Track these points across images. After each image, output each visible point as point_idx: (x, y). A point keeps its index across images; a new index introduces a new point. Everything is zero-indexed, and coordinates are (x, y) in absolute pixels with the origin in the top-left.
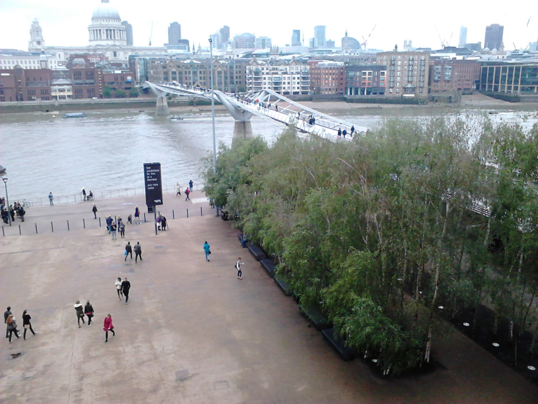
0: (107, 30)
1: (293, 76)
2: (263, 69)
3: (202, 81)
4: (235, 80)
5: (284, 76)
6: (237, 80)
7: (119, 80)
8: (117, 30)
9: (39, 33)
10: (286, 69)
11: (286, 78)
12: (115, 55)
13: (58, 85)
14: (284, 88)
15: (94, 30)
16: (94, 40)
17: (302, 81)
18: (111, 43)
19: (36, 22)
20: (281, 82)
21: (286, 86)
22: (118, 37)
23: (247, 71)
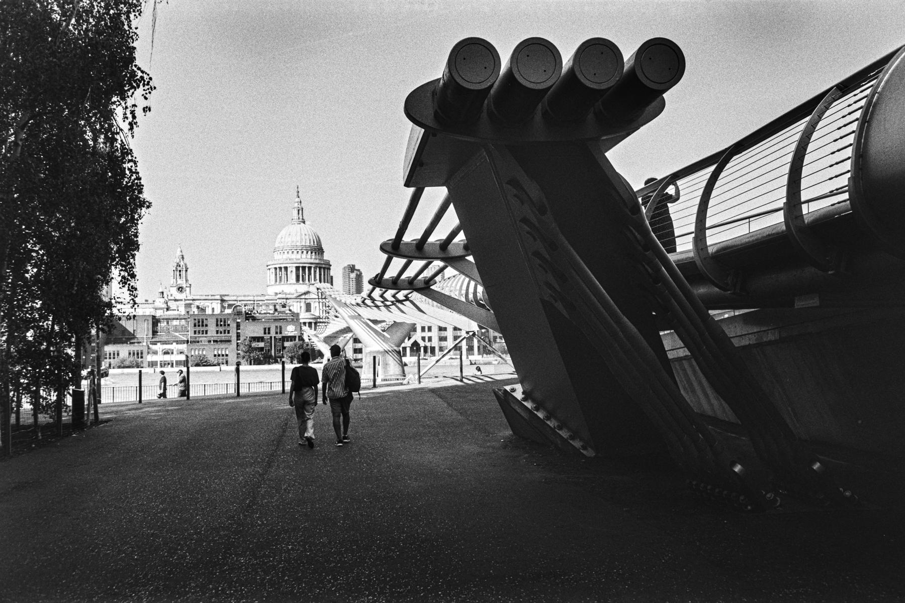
3: (427, 334)
7: (273, 334)
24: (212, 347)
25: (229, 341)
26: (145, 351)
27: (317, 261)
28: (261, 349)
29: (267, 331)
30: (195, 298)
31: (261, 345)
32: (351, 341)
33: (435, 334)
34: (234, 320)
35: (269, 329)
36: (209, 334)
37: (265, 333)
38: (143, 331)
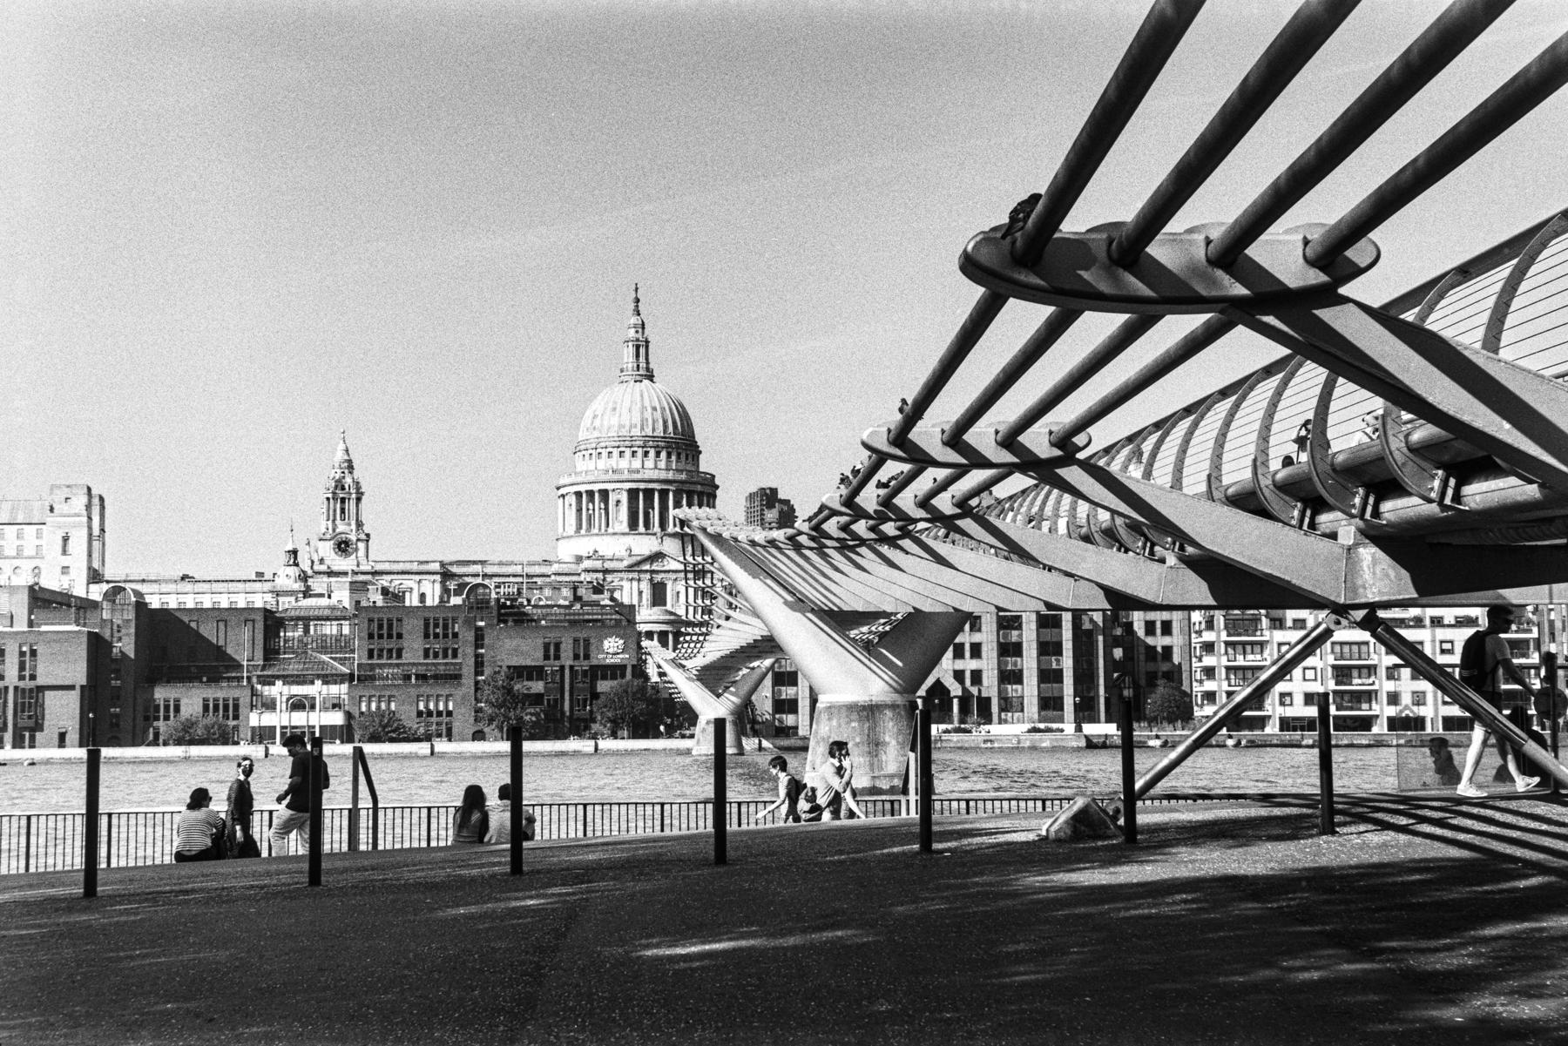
0: (633, 494)
1: (1442, 634)
3: (969, 664)
7: (567, 660)
12: (658, 596)
13: (289, 680)
14: (1394, 699)
15: (579, 494)
18: (644, 545)
24: (413, 692)
25: (457, 677)
26: (245, 700)
27: (683, 477)
28: (537, 699)
29: (552, 650)
30: (379, 567)
31: (538, 687)
32: (768, 681)
33: (988, 663)
34: (469, 622)
35: (557, 646)
36: (407, 657)
37: (547, 657)
38: (243, 647)
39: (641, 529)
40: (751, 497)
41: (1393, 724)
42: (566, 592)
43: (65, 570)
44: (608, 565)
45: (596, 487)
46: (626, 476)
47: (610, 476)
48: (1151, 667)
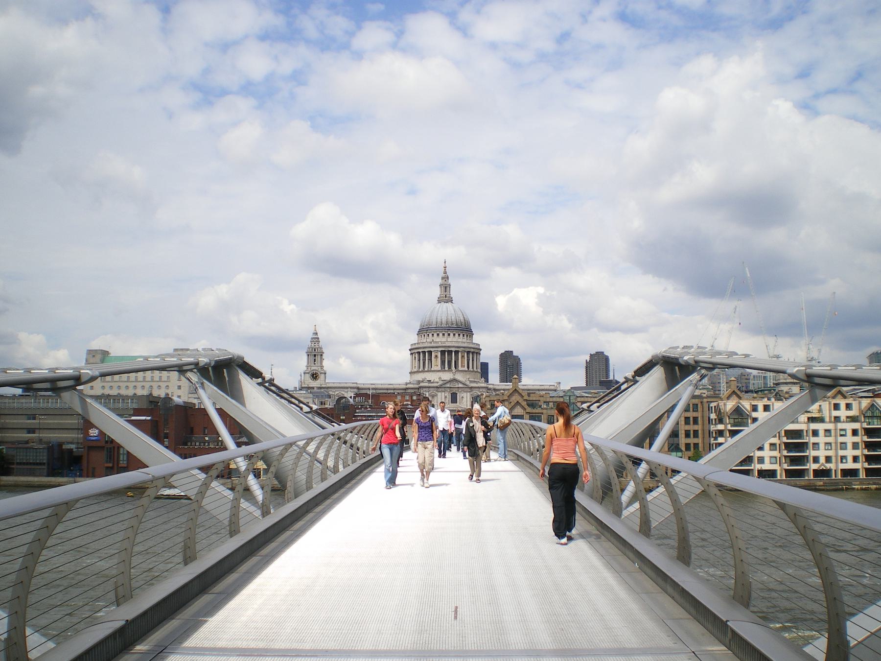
0: (443, 352)
1: (840, 426)
2: (755, 408)
4: (683, 441)
5: (814, 426)
6: (688, 441)
8: (463, 352)
9: (318, 358)
10: (820, 411)
11: (821, 433)
14: (816, 460)
15: (419, 353)
16: (418, 372)
17: (866, 439)
18: (447, 376)
19: (316, 339)
20: (807, 443)
21: (822, 453)
22: (463, 366)
23: (713, 416)
27: (466, 345)
39: (447, 368)
40: (502, 355)
41: (818, 473)
42: (407, 398)
43: (179, 387)
44: (430, 385)
45: (426, 350)
46: (440, 344)
47: (433, 345)
48: (688, 441)
